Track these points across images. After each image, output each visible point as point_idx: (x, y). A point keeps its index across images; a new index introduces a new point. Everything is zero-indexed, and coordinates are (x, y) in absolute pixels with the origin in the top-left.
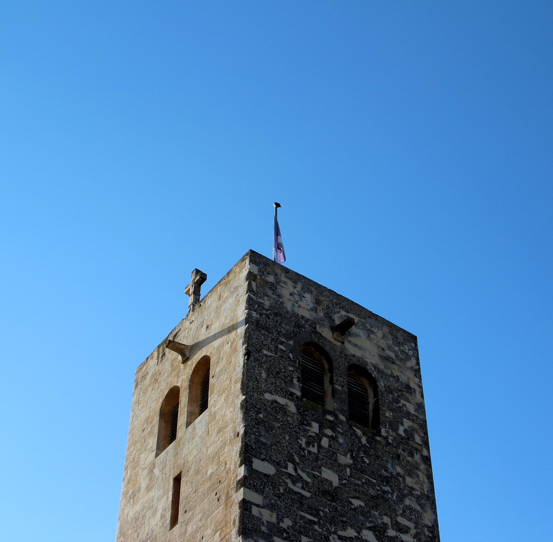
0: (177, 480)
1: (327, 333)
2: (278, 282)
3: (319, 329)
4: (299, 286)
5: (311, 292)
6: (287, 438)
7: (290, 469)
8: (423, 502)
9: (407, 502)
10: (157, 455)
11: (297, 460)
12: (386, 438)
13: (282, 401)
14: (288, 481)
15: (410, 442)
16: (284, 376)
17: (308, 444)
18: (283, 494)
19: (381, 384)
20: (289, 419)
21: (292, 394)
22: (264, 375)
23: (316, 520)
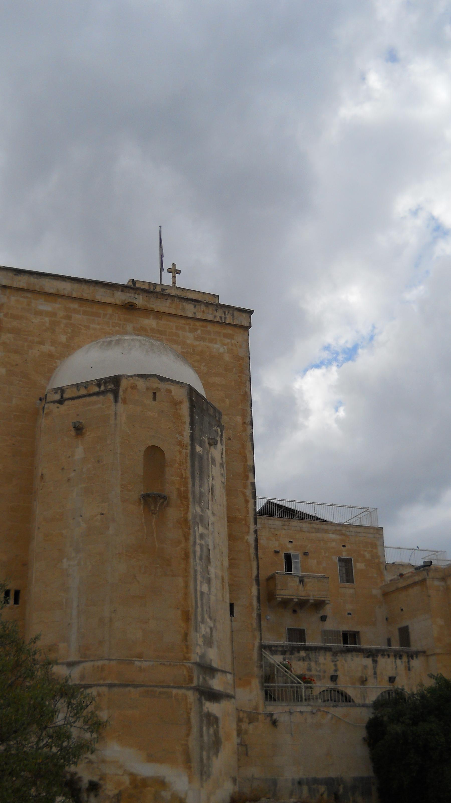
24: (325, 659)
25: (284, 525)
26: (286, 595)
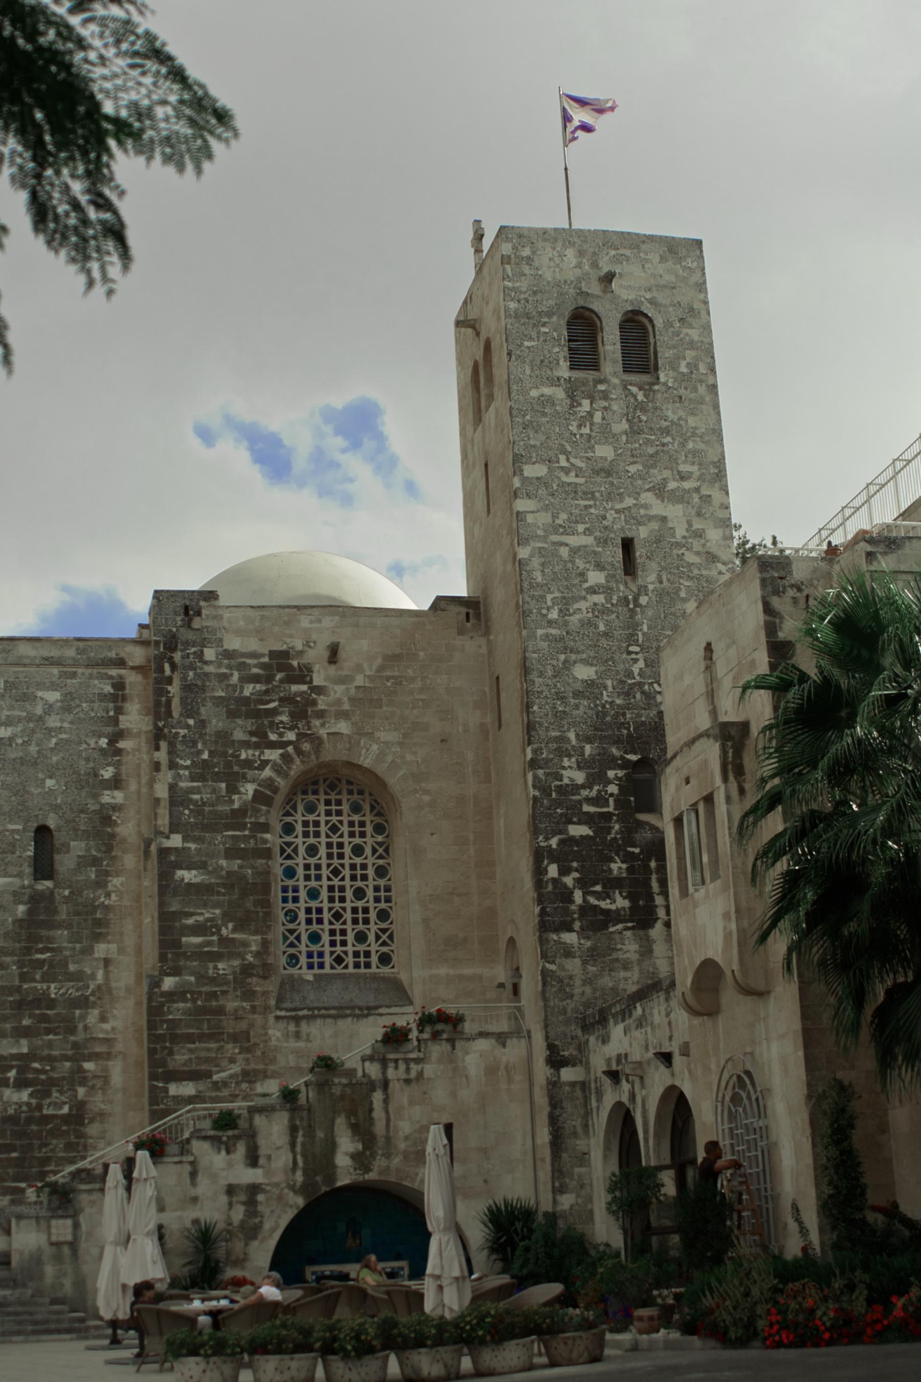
0: (486, 465)
3: (584, 289)
4: (560, 244)
5: (572, 244)
7: (563, 463)
9: (690, 445)
10: (475, 430)
11: (569, 449)
12: (665, 384)
13: (547, 391)
16: (549, 362)
17: (579, 426)
18: (557, 491)
20: (558, 408)
21: (558, 379)
22: (528, 372)
23: (591, 503)
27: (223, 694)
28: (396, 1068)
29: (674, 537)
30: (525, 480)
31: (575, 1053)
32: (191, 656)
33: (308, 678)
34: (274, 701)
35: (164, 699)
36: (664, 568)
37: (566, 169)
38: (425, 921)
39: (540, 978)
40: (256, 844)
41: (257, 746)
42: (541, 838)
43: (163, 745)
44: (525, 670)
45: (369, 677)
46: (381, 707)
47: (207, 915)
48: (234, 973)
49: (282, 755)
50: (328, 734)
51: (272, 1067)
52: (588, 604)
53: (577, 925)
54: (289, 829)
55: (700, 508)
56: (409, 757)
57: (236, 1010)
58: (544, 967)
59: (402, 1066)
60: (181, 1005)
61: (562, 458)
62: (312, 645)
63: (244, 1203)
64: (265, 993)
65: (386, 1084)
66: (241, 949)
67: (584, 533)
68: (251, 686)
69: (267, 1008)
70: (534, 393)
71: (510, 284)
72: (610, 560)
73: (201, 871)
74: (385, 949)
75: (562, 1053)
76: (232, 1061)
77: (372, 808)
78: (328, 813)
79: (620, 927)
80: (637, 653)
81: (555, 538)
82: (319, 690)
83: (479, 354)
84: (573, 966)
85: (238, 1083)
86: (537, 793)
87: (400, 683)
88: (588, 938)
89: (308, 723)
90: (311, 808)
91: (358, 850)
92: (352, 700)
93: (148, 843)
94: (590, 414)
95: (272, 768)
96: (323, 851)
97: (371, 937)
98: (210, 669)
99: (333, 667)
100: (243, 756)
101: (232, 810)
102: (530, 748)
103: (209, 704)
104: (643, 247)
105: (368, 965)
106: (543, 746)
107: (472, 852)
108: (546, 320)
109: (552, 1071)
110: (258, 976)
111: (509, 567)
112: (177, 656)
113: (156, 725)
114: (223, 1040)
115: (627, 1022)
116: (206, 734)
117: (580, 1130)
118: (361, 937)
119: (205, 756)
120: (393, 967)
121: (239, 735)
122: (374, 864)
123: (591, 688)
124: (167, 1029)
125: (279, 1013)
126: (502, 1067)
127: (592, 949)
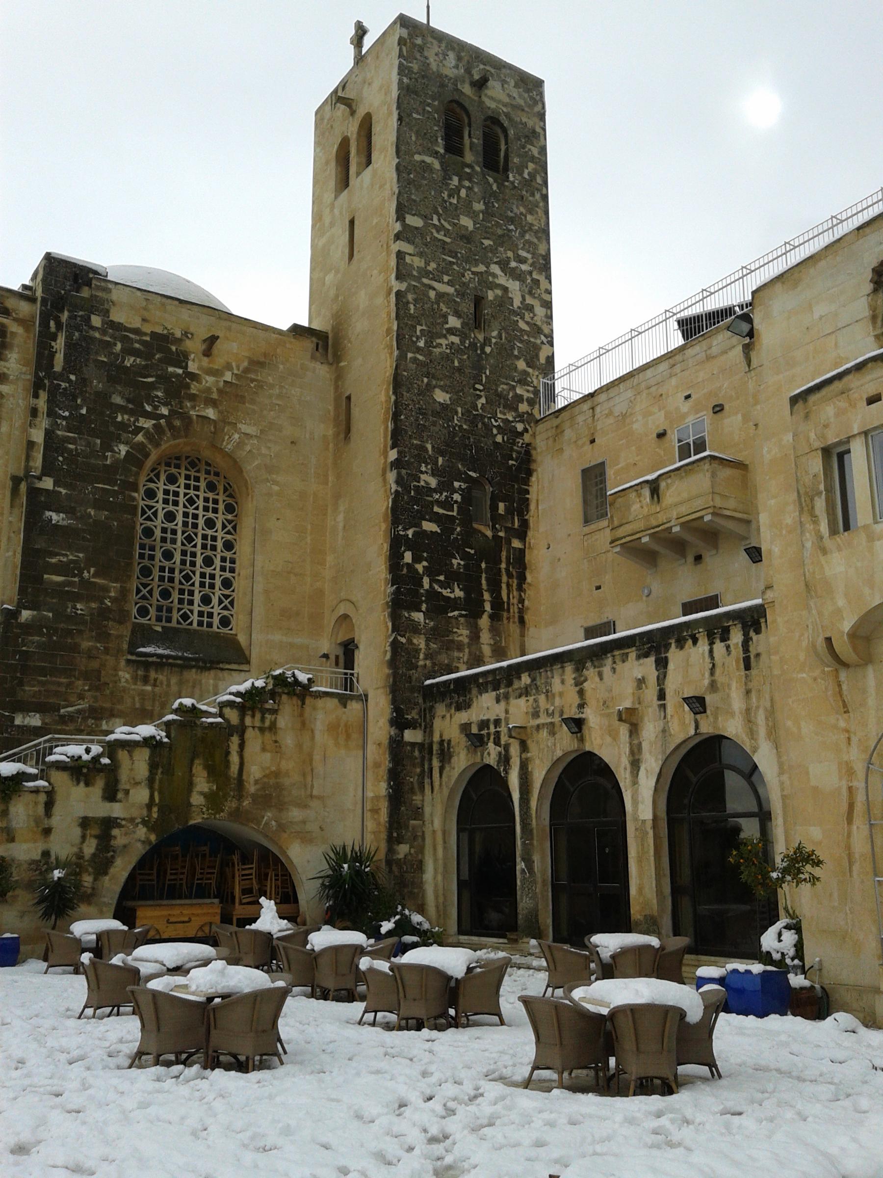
0: (352, 222)
1: (467, 89)
2: (425, 44)
3: (459, 86)
4: (443, 45)
5: (453, 49)
6: (433, 193)
7: (436, 221)
8: (540, 235)
9: (527, 237)
10: (336, 197)
11: (441, 212)
12: (513, 183)
13: (428, 160)
14: (434, 231)
15: (533, 184)
17: (450, 196)
19: (511, 132)
21: (437, 153)
22: (414, 138)
23: (454, 260)
24: (563, 682)
25: (674, 365)
26: (625, 537)
27: (105, 360)
28: (253, 716)
29: (512, 305)
30: (405, 226)
31: (416, 717)
32: (79, 319)
33: (184, 364)
34: (152, 377)
35: (46, 352)
36: (504, 328)
37: (428, 7)
38: (266, 592)
39: (388, 648)
40: (124, 499)
41: (131, 413)
42: (400, 528)
43: (43, 396)
44: (397, 383)
45: (236, 375)
46: (244, 403)
47: (71, 557)
48: (92, 615)
49: (154, 425)
50: (197, 416)
51: (119, 707)
52: (447, 342)
53: (424, 607)
54: (151, 494)
55: (531, 288)
56: (264, 451)
57: (90, 649)
58: (395, 638)
59: (258, 716)
60: (37, 638)
61: (435, 217)
62: (190, 336)
63: (96, 837)
64: (120, 637)
65: (241, 730)
66: (101, 594)
67: (447, 283)
68: (132, 359)
69: (119, 651)
70: (417, 157)
71: (405, 62)
72: (466, 310)
73: (69, 515)
74: (226, 613)
75: (406, 716)
76: (81, 697)
77: (225, 490)
78: (187, 487)
79: (456, 613)
80: (480, 391)
81: (425, 281)
82: (194, 377)
83: (352, 129)
84: (420, 642)
85: (85, 719)
86: (400, 489)
87: (262, 387)
88: (431, 619)
89: (181, 403)
90: (172, 480)
91: (210, 524)
92: (220, 391)
93: (16, 481)
94: (457, 190)
95: (145, 435)
96: (180, 519)
97: (215, 601)
98: (97, 335)
99: (206, 360)
100: (119, 419)
101: (105, 465)
102: (395, 450)
103: (92, 365)
104: (504, 70)
105: (210, 625)
106: (406, 450)
107: (309, 540)
108: (429, 101)
109: (397, 731)
110: (114, 620)
111: (380, 300)
112: (65, 316)
113: (36, 375)
114: (75, 676)
115: (502, 691)
116: (86, 391)
117: (416, 786)
118: (206, 600)
119: (84, 411)
120: (231, 629)
121: (117, 400)
122: (222, 538)
123: (445, 410)
124: (19, 660)
125: (130, 657)
126: (342, 725)
127: (433, 629)
